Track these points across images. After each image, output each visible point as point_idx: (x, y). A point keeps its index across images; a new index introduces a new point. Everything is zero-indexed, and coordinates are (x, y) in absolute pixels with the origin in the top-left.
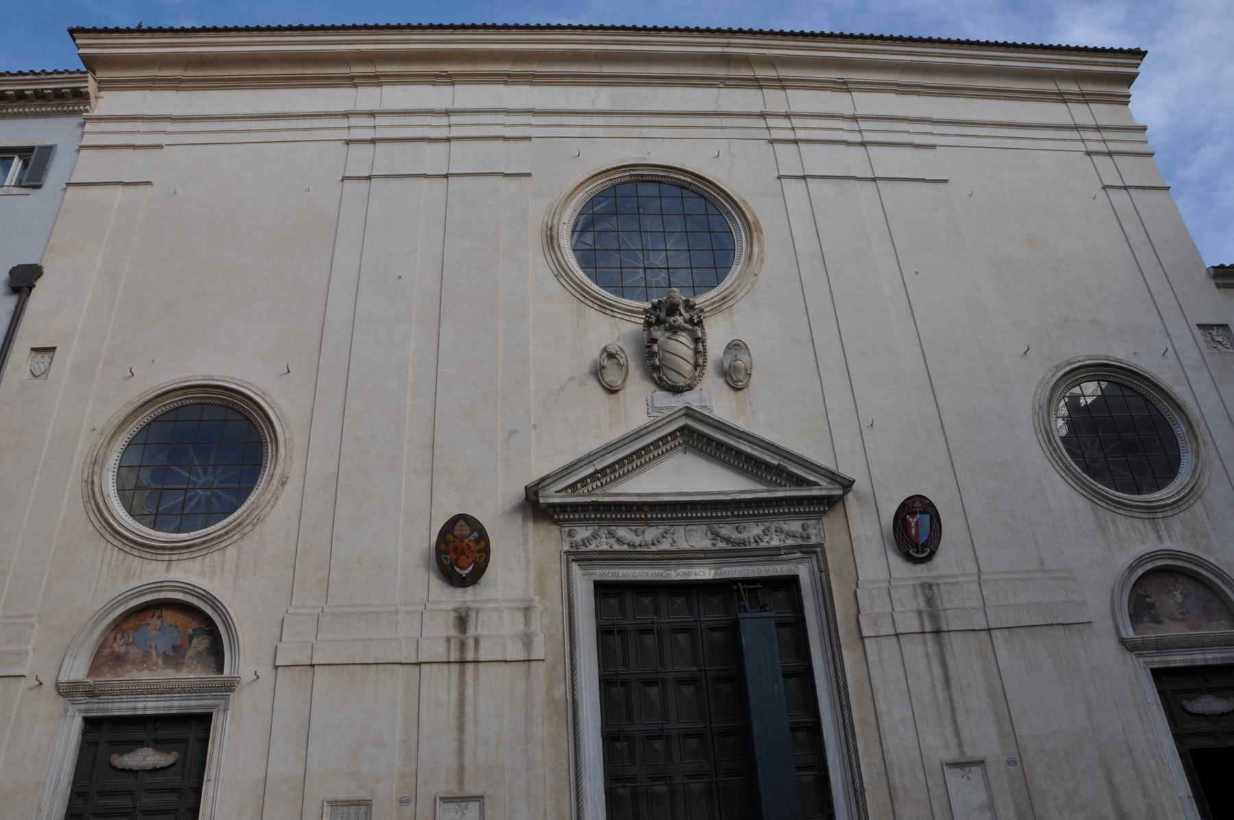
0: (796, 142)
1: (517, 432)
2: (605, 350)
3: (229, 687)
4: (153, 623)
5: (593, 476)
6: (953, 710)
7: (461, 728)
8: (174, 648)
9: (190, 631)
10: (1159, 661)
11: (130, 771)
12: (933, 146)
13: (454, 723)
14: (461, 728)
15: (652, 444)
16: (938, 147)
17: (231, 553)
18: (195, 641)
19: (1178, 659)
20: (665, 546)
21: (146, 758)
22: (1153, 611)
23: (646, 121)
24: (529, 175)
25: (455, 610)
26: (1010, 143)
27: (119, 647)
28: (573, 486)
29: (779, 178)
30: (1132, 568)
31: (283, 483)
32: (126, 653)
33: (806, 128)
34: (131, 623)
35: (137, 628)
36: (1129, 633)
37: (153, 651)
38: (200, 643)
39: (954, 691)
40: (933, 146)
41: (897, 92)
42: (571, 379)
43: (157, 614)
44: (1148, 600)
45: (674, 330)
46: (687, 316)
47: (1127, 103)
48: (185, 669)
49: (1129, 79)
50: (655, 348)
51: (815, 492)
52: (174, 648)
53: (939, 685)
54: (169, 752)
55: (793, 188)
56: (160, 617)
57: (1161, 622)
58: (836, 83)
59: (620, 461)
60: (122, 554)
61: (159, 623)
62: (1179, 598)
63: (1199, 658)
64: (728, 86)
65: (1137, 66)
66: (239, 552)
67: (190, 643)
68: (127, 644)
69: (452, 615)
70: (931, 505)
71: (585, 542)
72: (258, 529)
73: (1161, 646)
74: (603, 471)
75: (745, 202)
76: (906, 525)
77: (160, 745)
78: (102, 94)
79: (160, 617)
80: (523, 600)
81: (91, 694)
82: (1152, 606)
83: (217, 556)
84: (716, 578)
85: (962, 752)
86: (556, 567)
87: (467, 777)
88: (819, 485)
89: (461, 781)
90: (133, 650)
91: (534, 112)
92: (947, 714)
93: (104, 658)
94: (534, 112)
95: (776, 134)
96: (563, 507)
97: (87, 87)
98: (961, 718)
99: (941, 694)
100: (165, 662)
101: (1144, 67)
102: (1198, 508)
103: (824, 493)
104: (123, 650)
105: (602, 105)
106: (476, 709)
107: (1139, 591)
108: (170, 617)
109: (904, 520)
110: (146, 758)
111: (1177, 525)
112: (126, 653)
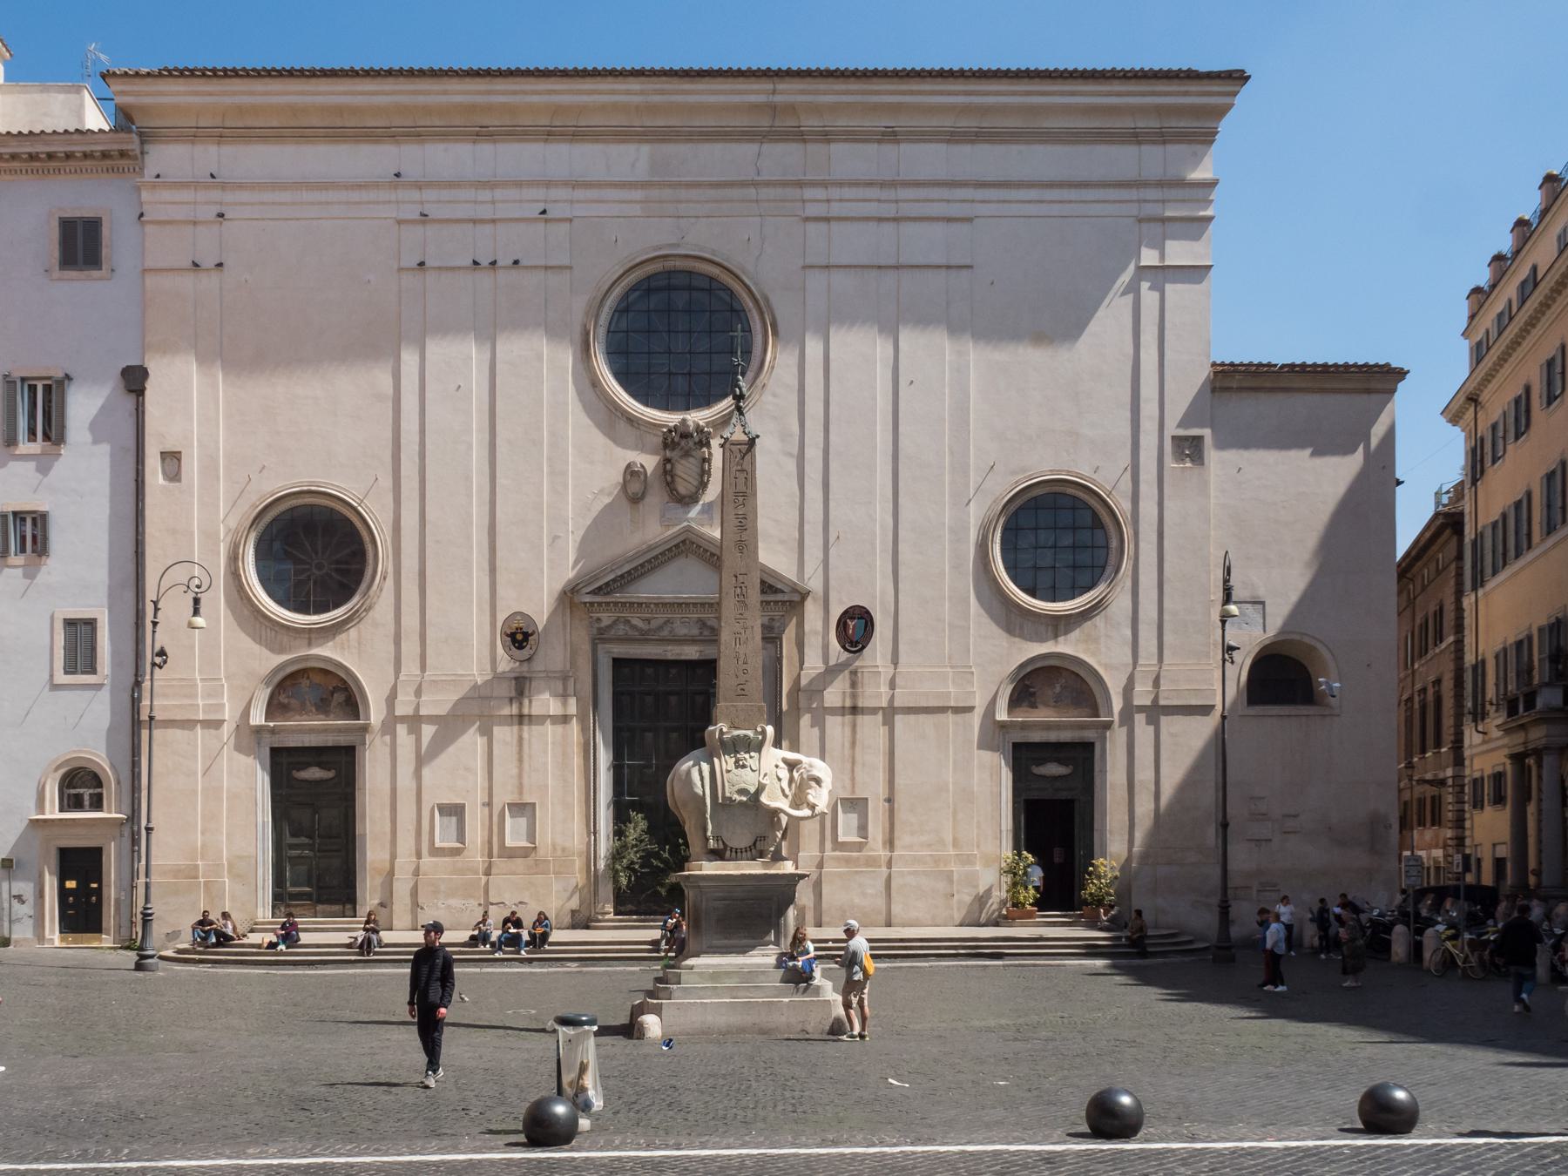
0: (827, 220)
1: (559, 537)
2: (629, 466)
3: (365, 729)
4: (305, 683)
5: (614, 580)
6: (853, 763)
7: (520, 760)
8: (322, 700)
9: (331, 688)
10: (1019, 737)
11: (306, 781)
12: (969, 220)
13: (517, 756)
14: (520, 760)
15: (660, 554)
16: (976, 220)
17: (353, 633)
18: (335, 695)
19: (1037, 737)
20: (665, 633)
21: (314, 773)
22: (1033, 699)
23: (683, 194)
24: (570, 268)
25: (516, 679)
26: (1056, 209)
27: (283, 699)
28: (600, 588)
29: (804, 267)
30: (1022, 666)
31: (385, 578)
32: (289, 703)
33: (841, 200)
34: (288, 683)
35: (294, 685)
36: (1002, 715)
37: (308, 702)
38: (339, 697)
39: (858, 749)
40: (969, 220)
41: (948, 141)
42: (601, 491)
43: (306, 676)
44: (1031, 690)
45: (687, 454)
46: (697, 440)
47: (1212, 142)
48: (332, 716)
49: (1221, 112)
50: (669, 467)
51: (779, 597)
52: (322, 700)
53: (847, 745)
54: (329, 770)
55: (816, 281)
56: (308, 678)
57: (1036, 707)
58: (883, 134)
59: (635, 569)
60: (273, 633)
61: (308, 682)
62: (1058, 689)
63: (1053, 737)
64: (771, 141)
65: (1235, 94)
66: (359, 632)
67: (332, 695)
68: (288, 697)
69: (513, 682)
70: (868, 612)
71: (609, 627)
72: (371, 613)
73: (1024, 726)
74: (622, 576)
75: (767, 300)
76: (845, 625)
77: (321, 765)
78: (147, 147)
79: (308, 678)
80: (561, 671)
81: (273, 731)
82: (1033, 694)
83: (344, 636)
84: (701, 658)
85: (853, 792)
86: (586, 647)
87: (526, 789)
88: (783, 592)
89: (521, 793)
90: (293, 701)
91: (575, 185)
92: (848, 766)
93: (274, 708)
94: (575, 185)
95: (813, 210)
96: (592, 604)
97: (133, 150)
98: (858, 769)
99: (847, 752)
100: (317, 710)
101: (1245, 97)
102: (1098, 621)
103: (786, 598)
104: (286, 701)
105: (641, 173)
106: (530, 747)
107: (1027, 682)
108: (317, 679)
109: (845, 623)
110: (314, 773)
111: (1076, 634)
112: (289, 703)
